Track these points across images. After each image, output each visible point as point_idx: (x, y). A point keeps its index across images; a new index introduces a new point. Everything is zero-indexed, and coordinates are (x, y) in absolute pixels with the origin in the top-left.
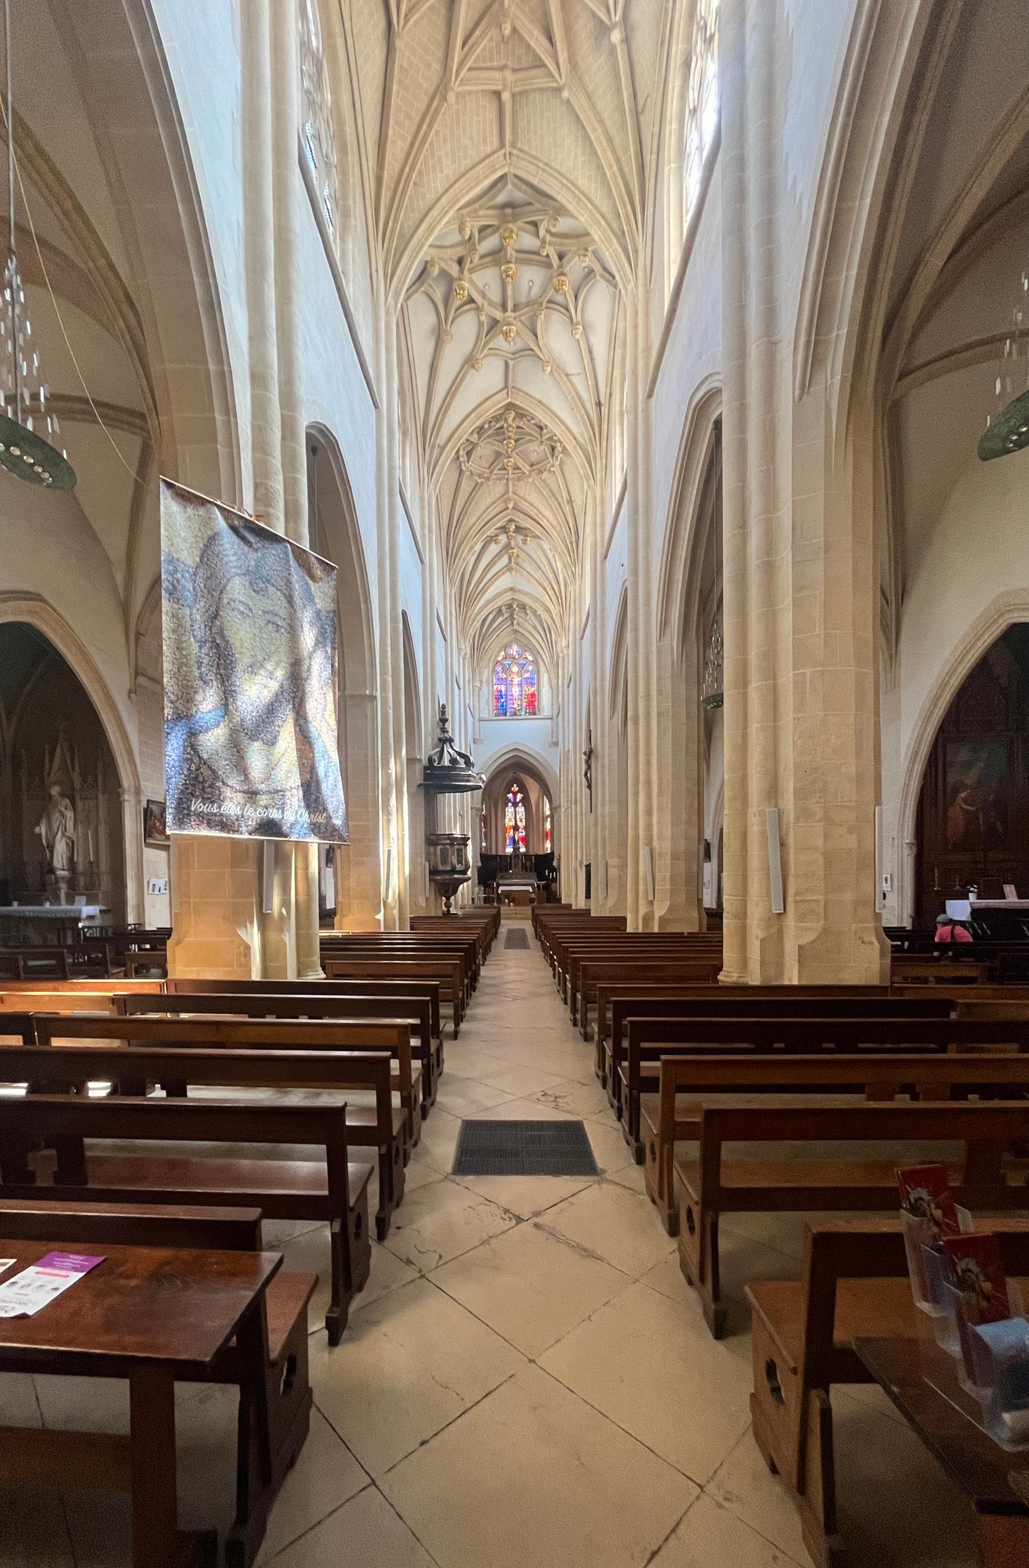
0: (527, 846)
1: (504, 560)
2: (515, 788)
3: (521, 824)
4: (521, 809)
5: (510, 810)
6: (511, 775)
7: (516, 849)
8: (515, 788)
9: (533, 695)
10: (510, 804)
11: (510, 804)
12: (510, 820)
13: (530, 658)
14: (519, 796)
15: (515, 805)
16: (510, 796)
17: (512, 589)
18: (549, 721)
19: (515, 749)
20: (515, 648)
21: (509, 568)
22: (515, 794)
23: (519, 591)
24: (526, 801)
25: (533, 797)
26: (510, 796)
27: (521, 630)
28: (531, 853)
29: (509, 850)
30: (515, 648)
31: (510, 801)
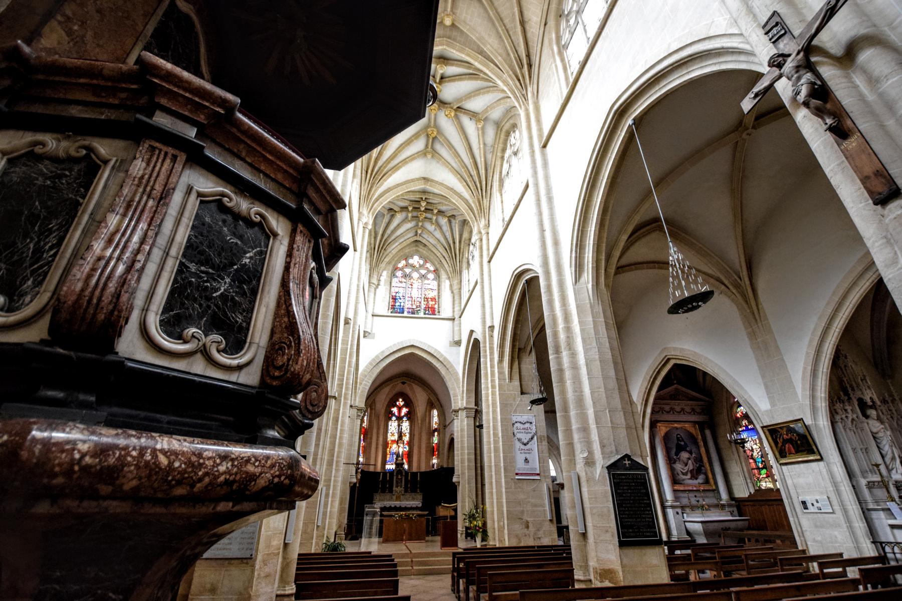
0: (410, 463)
1: (419, 145)
2: (401, 402)
3: (406, 439)
4: (406, 425)
5: (393, 425)
6: (399, 387)
7: (399, 465)
8: (401, 402)
9: (433, 299)
10: (394, 418)
11: (394, 418)
12: (393, 435)
13: (432, 269)
14: (404, 411)
15: (399, 418)
16: (395, 410)
17: (424, 178)
18: (449, 323)
19: (412, 346)
20: (416, 258)
21: (423, 154)
22: (400, 409)
23: (432, 181)
24: (410, 416)
25: (420, 409)
26: (395, 410)
27: (424, 241)
28: (415, 470)
29: (390, 467)
30: (416, 258)
31: (393, 415)
